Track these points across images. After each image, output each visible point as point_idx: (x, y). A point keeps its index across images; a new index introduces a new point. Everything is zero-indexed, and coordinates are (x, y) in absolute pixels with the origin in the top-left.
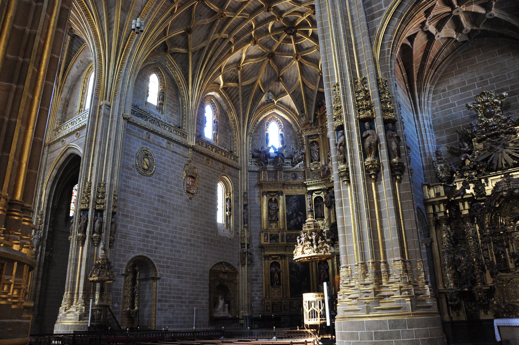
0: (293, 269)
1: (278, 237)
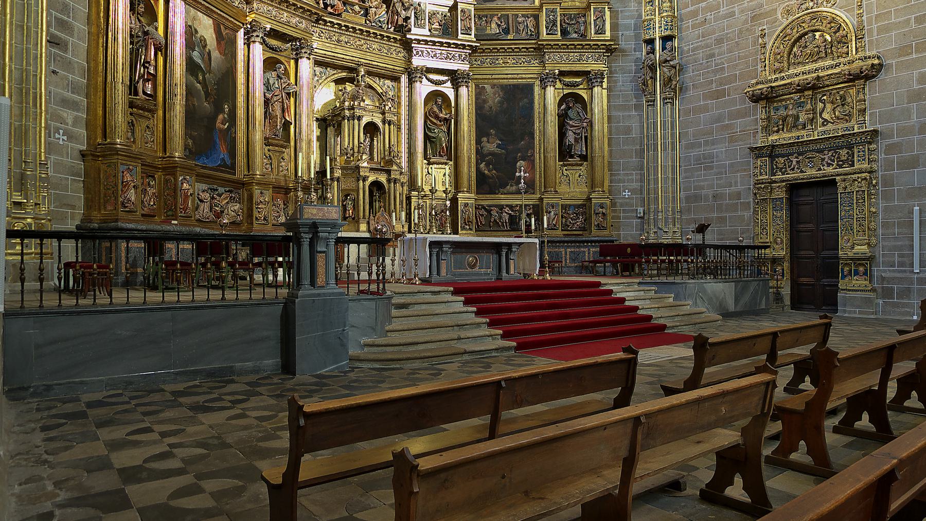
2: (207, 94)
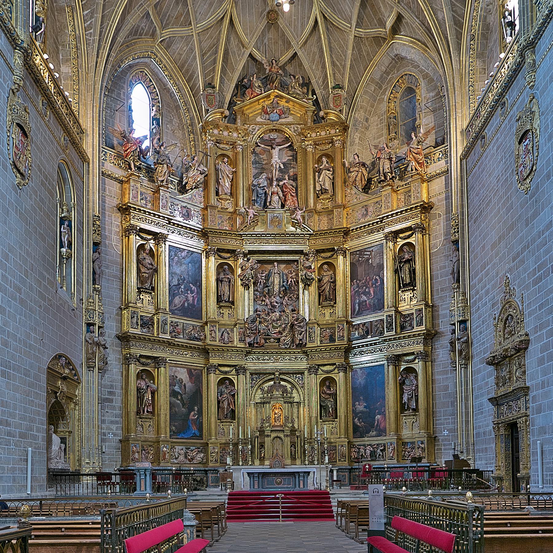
0: (177, 388)
1: (153, 325)
2: (184, 405)
